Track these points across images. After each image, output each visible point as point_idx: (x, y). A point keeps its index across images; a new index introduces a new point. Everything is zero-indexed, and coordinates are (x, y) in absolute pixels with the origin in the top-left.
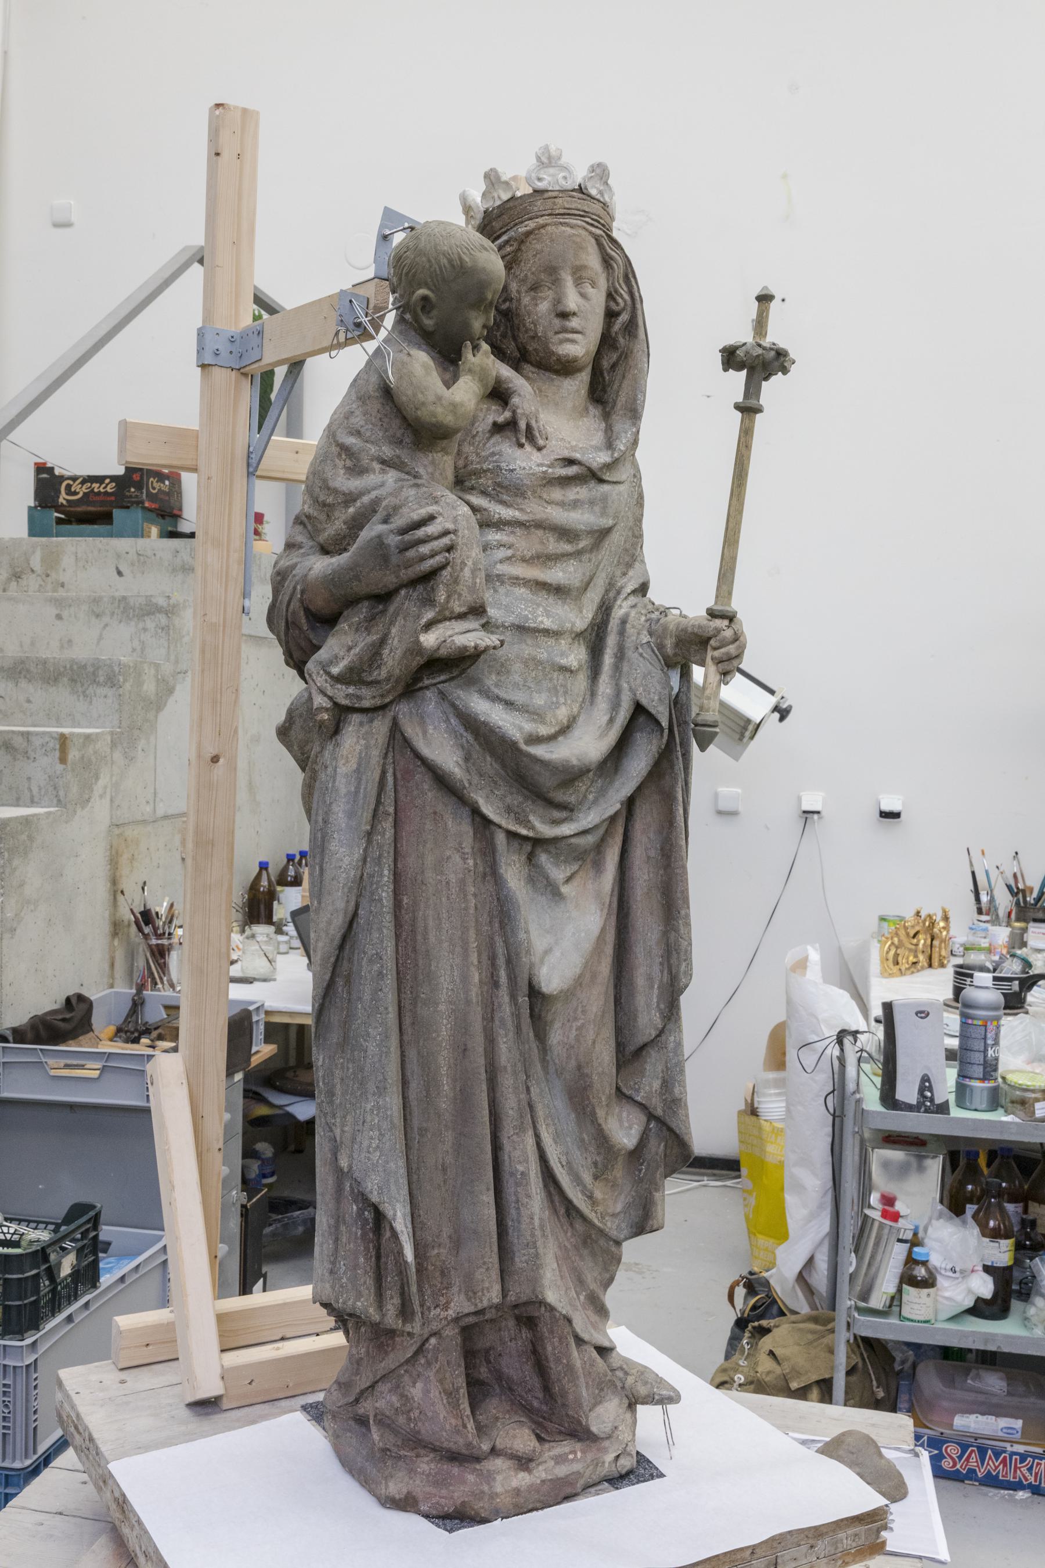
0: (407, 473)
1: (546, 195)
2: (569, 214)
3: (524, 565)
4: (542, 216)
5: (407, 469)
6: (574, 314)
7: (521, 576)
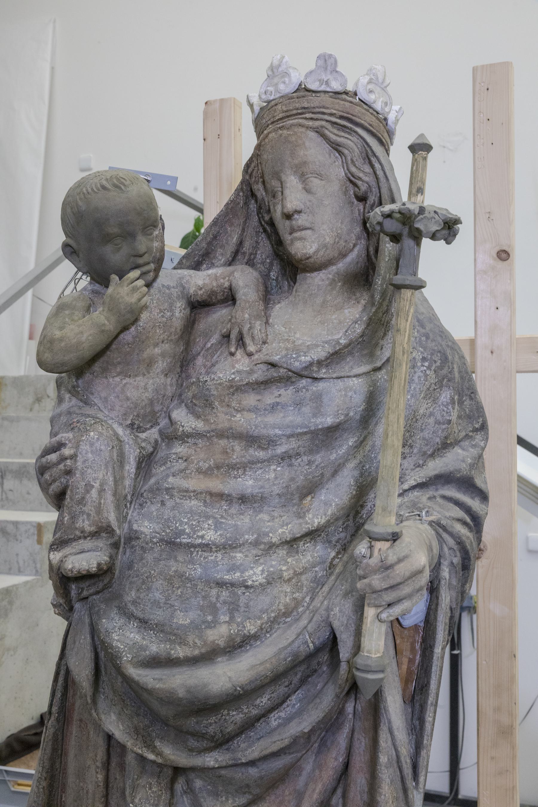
0: (81, 400)
1: (270, 105)
2: (288, 117)
3: (201, 476)
4: (268, 126)
5: (80, 397)
6: (299, 212)
7: (191, 489)
